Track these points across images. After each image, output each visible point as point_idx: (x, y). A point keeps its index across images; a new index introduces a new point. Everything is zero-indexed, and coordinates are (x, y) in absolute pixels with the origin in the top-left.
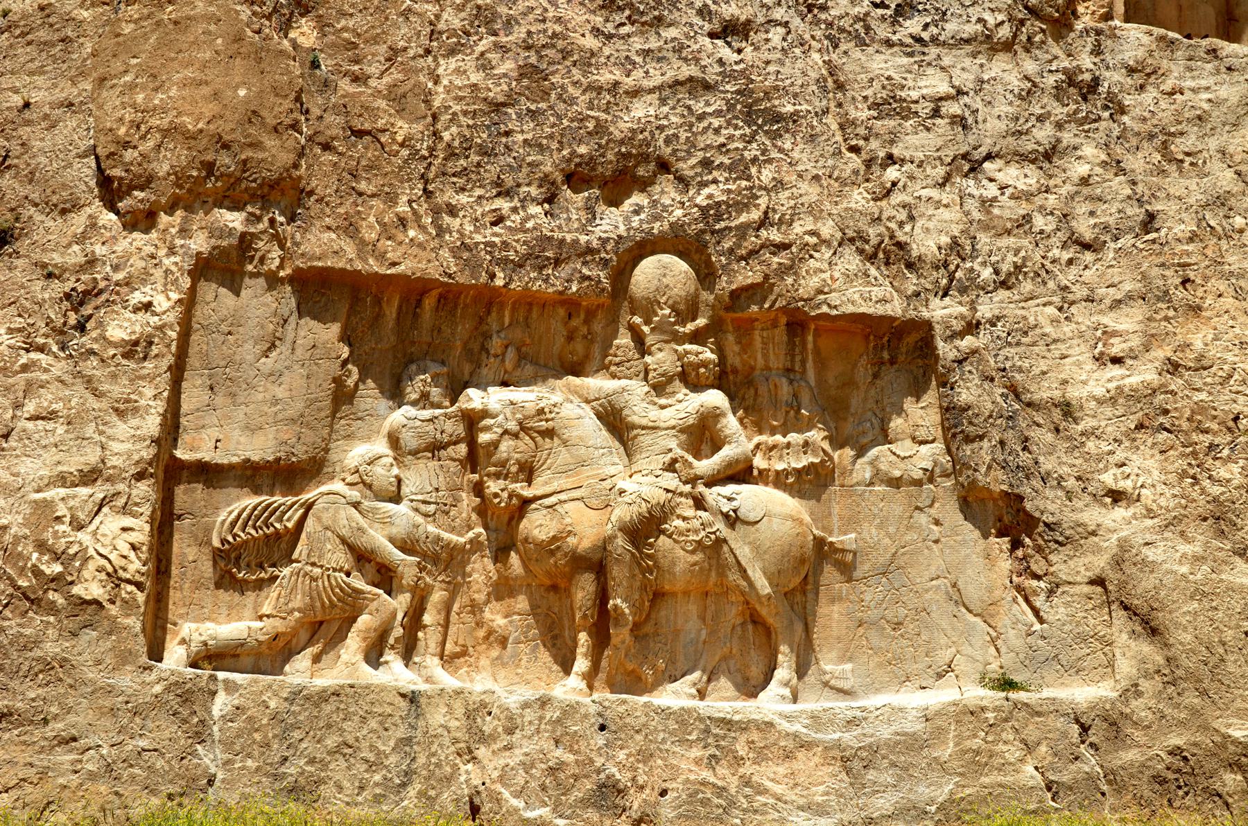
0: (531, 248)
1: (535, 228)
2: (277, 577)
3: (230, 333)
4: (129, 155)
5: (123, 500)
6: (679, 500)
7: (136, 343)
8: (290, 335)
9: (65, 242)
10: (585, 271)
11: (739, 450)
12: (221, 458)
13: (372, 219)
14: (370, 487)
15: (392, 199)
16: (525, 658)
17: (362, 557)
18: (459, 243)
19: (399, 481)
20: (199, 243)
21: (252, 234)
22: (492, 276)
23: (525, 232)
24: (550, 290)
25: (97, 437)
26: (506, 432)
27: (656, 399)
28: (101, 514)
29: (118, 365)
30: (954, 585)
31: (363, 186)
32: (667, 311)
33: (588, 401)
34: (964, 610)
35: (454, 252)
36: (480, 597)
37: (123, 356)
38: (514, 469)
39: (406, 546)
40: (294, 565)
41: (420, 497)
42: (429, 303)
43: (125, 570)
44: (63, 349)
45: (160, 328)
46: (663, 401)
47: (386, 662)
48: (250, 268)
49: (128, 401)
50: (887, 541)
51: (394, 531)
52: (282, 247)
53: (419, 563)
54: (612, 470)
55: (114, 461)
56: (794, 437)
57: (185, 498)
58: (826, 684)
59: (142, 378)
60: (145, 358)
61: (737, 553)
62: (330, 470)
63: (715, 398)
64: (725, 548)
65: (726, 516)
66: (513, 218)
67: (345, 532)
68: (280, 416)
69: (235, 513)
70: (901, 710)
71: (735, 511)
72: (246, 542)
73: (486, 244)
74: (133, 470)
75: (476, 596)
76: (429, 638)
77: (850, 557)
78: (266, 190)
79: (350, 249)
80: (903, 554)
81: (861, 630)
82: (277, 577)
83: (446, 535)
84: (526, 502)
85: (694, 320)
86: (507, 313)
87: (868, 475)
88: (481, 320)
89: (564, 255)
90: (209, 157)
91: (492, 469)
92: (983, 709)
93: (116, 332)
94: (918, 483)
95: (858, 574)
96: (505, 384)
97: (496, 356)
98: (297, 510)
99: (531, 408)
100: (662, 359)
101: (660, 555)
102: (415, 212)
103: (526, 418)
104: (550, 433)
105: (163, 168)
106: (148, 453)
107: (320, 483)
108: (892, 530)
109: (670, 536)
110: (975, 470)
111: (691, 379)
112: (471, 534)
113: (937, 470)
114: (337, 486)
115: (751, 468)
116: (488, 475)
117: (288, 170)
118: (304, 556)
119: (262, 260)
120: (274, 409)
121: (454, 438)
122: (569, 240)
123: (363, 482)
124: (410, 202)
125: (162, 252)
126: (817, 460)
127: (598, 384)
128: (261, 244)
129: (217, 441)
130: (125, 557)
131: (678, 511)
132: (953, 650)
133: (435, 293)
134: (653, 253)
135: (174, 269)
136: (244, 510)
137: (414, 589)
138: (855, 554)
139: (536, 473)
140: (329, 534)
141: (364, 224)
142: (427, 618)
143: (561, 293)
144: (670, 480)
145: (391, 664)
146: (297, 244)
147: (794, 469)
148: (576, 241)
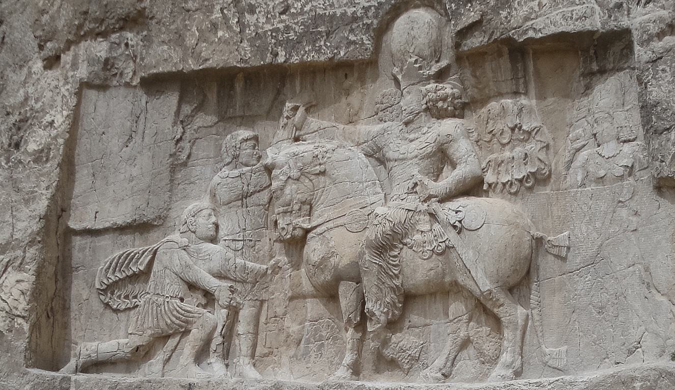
0: (308, 27)
1: (311, 10)
2: (138, 305)
3: (104, 133)
4: (45, 18)
5: (19, 262)
6: (417, 218)
7: (42, 151)
8: (141, 127)
9: (16, 87)
10: (352, 38)
11: (468, 168)
12: (99, 226)
13: (194, 28)
14: (194, 232)
15: (210, 10)
16: (313, 355)
17: (192, 286)
18: (254, 34)
19: (217, 226)
20: (83, 72)
21: (115, 58)
22: (277, 55)
23: (303, 15)
24: (322, 58)
25: (11, 220)
26: (289, 177)
27: (407, 135)
28: (7, 273)
29: (31, 168)
30: (647, 269)
31: (190, 5)
32: (413, 60)
33: (358, 144)
34: (654, 291)
35: (251, 41)
36: (280, 311)
37: (33, 162)
38: (296, 207)
39: (220, 276)
40: (148, 296)
41: (231, 237)
42: (239, 86)
43: (17, 309)
44: (8, 162)
45: (55, 138)
46: (412, 136)
47: (211, 363)
48: (115, 83)
49: (33, 192)
50: (595, 235)
51: (212, 266)
52: (135, 62)
53: (230, 287)
54: (373, 199)
55: (18, 236)
56: (519, 151)
57: (80, 255)
58: (545, 364)
59: (42, 175)
60: (47, 160)
61: (463, 258)
62: (172, 224)
63: (449, 126)
64: (454, 254)
65: (455, 227)
66: (296, 6)
67: (177, 269)
68: (135, 189)
69: (108, 263)
70: (571, 383)
71: (460, 222)
72: (116, 282)
73: (272, 31)
74: (28, 239)
75: (278, 310)
76: (242, 344)
77: (564, 254)
78: (121, 23)
79: (176, 55)
80: (608, 245)
81: (575, 316)
82: (138, 306)
83: (250, 264)
84: (307, 231)
85: (437, 62)
86: (298, 83)
87: (579, 178)
88: (279, 92)
89: (334, 27)
90: (84, 9)
91: (281, 209)
92: (633, 379)
93: (32, 147)
94: (621, 177)
95: (568, 266)
96: (297, 139)
97: (288, 118)
98: (147, 256)
99: (308, 157)
100: (411, 100)
101: (404, 264)
102: (225, 17)
103: (304, 165)
104: (323, 173)
105: (61, 24)
106: (35, 226)
107: (165, 235)
108: (598, 224)
109: (411, 248)
110: (663, 162)
111: (435, 111)
112: (272, 262)
113: (637, 167)
114: (176, 236)
115: (482, 182)
116: (279, 214)
117: (133, 5)
118: (152, 290)
119: (121, 74)
120: (132, 184)
121: (258, 188)
122: (349, 14)
123: (190, 230)
124: (222, 10)
125: (61, 84)
126: (533, 170)
127: (367, 128)
128: (120, 64)
129: (96, 213)
130: (17, 300)
131: (419, 227)
132: (643, 328)
133: (240, 75)
134: (407, 10)
135: (67, 94)
136: (114, 259)
137: (229, 307)
138: (569, 248)
139: (314, 208)
140: (168, 271)
141: (188, 34)
142: (242, 327)
143: (331, 59)
144: (413, 202)
145: (214, 365)
146: (142, 59)
147: (516, 179)
148: (344, 14)
